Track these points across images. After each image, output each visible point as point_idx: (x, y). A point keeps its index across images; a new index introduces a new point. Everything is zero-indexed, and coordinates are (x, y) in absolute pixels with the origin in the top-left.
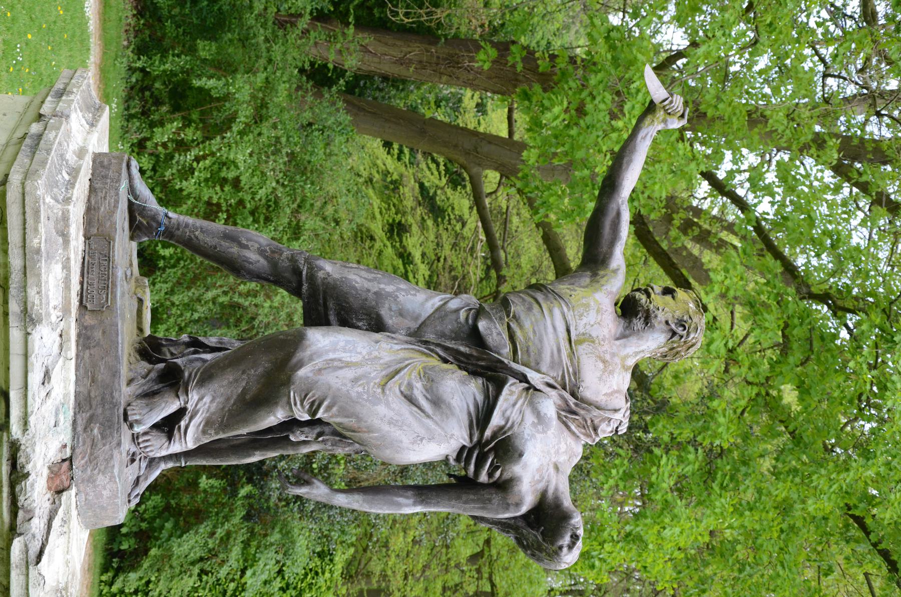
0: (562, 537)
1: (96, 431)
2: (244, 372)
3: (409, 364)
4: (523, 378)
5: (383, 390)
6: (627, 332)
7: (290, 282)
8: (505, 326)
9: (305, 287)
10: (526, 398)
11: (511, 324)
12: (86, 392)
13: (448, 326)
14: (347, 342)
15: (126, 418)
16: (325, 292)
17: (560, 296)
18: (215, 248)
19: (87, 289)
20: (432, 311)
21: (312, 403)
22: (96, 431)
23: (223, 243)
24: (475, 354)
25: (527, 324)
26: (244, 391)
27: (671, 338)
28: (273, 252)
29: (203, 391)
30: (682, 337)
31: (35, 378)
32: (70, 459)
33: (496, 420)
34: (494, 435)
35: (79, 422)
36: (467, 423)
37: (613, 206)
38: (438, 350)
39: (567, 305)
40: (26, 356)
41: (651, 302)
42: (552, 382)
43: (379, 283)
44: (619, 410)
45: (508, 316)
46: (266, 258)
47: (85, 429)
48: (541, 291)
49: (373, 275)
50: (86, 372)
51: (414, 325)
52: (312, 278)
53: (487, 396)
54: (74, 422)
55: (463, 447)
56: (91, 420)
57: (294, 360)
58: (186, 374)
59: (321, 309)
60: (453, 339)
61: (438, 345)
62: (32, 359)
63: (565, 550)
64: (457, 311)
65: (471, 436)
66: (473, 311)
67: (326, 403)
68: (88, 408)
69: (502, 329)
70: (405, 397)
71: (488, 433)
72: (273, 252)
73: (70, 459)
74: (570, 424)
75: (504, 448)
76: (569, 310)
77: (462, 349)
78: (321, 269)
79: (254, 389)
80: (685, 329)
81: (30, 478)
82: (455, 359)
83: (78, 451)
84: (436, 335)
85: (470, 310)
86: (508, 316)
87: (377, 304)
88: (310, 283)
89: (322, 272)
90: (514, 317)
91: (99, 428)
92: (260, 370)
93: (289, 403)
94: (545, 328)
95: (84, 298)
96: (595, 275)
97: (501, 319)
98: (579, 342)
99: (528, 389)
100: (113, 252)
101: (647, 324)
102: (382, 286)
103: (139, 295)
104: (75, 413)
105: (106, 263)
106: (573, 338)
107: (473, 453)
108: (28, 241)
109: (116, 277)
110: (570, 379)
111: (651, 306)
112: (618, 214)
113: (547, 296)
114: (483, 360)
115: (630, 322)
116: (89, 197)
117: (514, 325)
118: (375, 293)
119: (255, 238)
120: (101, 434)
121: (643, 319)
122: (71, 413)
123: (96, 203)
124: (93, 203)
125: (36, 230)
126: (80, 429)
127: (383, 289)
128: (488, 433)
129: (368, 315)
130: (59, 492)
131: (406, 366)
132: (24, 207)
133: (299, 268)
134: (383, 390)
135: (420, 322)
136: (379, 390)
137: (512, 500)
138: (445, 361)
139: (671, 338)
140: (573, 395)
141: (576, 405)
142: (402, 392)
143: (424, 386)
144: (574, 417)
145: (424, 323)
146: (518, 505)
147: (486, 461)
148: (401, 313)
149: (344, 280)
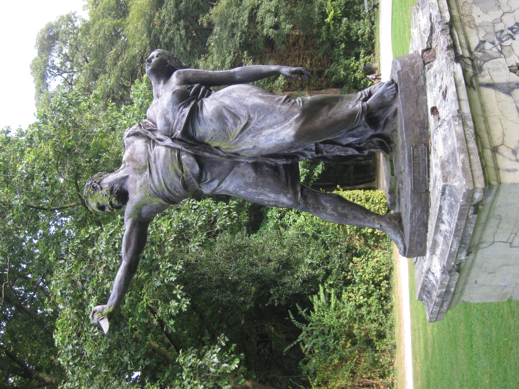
0: (156, 61)
1: (412, 77)
2: (330, 117)
3: (236, 138)
4: (173, 140)
5: (249, 116)
6: (122, 181)
7: (308, 192)
8: (184, 171)
9: (299, 189)
10: (172, 129)
11: (181, 172)
12: (420, 96)
13: (217, 170)
14: (270, 140)
15: (396, 86)
16: (287, 185)
17: (155, 193)
18: (352, 209)
19: (425, 156)
20: (227, 179)
21: (289, 101)
22: (412, 77)
23: (348, 212)
24: (201, 152)
25: (172, 174)
26: (330, 109)
27: (100, 182)
28: (318, 208)
29: (354, 109)
30: (95, 182)
31: (452, 89)
32: (425, 64)
33: (187, 111)
34: (188, 104)
35: (422, 81)
36: (204, 108)
37: (129, 255)
38: (222, 154)
39: (151, 188)
40: (459, 100)
41: (110, 199)
42: (159, 142)
43: (257, 192)
44: (127, 137)
45: (183, 177)
46: (322, 204)
47: (418, 78)
48: (166, 198)
49: (260, 197)
50: (422, 107)
51: (236, 169)
52: (295, 194)
53: (193, 125)
54: (425, 80)
55: (207, 97)
56: (416, 82)
57: (301, 122)
58: (364, 119)
59: (289, 177)
60: (214, 162)
61: (222, 156)
62: (454, 98)
63: (155, 56)
64: (212, 180)
65: (202, 103)
66: (203, 180)
67: (282, 101)
68: (418, 88)
69: (186, 168)
70: (238, 117)
71: (192, 103)
72: (318, 208)
73: (425, 64)
74: (152, 124)
75: (182, 98)
76: (150, 186)
77: (208, 155)
78: (289, 199)
79: (324, 110)
80: (93, 186)
81: (446, 46)
82: (212, 150)
83: (421, 68)
84: (223, 163)
85: (205, 181)
86: (183, 177)
87: (257, 179)
88: (296, 190)
89: (289, 197)
90: (179, 177)
91: (411, 79)
92: (321, 118)
93: (303, 102)
94: (162, 172)
95: (426, 151)
96: (140, 215)
97: (187, 175)
98: (145, 168)
99: (172, 136)
100: (411, 183)
101: (112, 187)
102: (254, 191)
103: (394, 177)
104: (425, 84)
105: (416, 174)
106: (148, 170)
107: (201, 95)
108: (467, 156)
109: (409, 166)
110: (150, 145)
111: (109, 196)
112: (127, 250)
113: (163, 193)
114: (196, 149)
115: (121, 187)
116: (427, 220)
117: (180, 172)
118: (258, 186)
119: (329, 217)
120: (409, 76)
121: (114, 189)
122: (427, 84)
123: (424, 216)
124: (425, 215)
125: (463, 163)
126: (422, 77)
127: (253, 189)
128: (192, 103)
129: (262, 173)
130: (428, 49)
131: (237, 136)
132: (472, 174)
133: (303, 199)
134: (249, 116)
135: (233, 172)
136: (252, 116)
137: (182, 76)
138: (217, 148)
139: (100, 182)
140: (149, 139)
141: (148, 133)
142: (240, 119)
143: (227, 126)
144: (149, 128)
145: (231, 171)
146: (179, 73)
147: (194, 91)
148: (243, 175)
149: (277, 193)
